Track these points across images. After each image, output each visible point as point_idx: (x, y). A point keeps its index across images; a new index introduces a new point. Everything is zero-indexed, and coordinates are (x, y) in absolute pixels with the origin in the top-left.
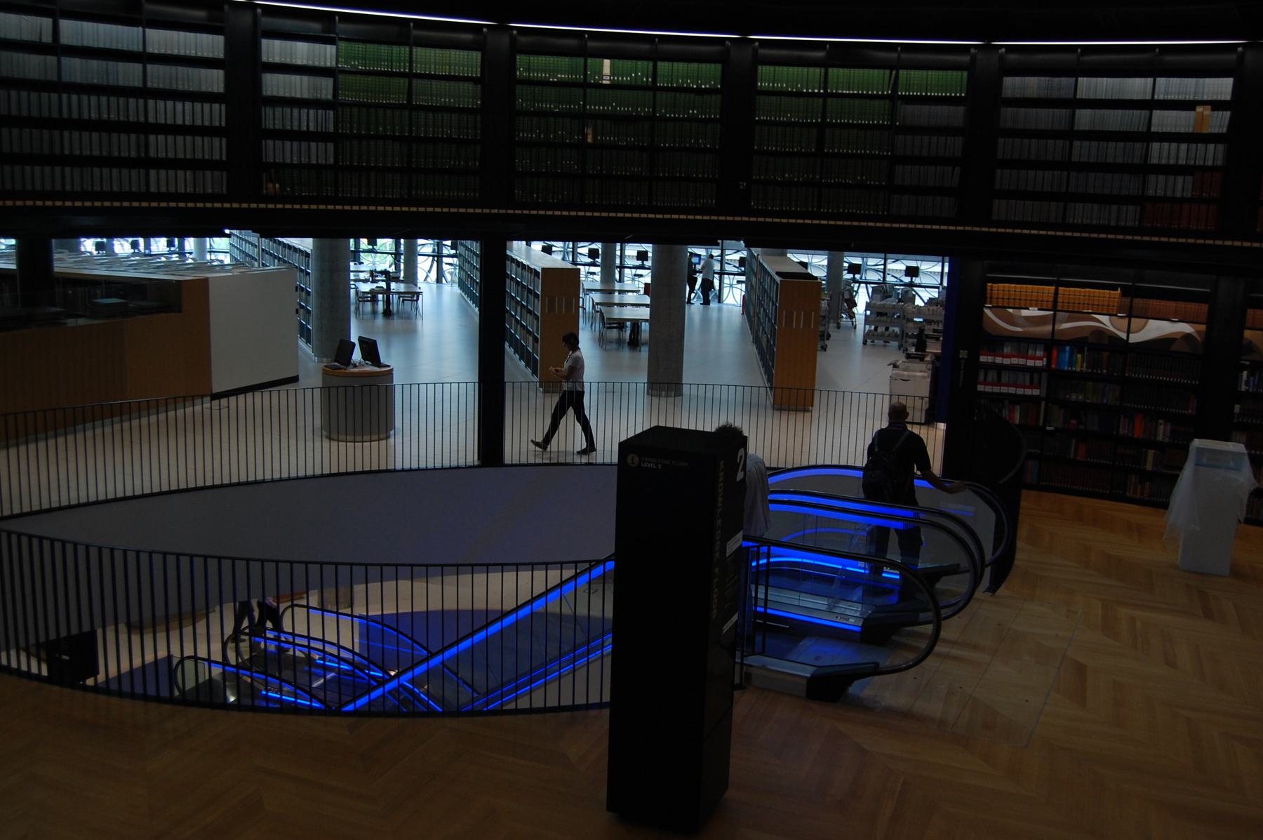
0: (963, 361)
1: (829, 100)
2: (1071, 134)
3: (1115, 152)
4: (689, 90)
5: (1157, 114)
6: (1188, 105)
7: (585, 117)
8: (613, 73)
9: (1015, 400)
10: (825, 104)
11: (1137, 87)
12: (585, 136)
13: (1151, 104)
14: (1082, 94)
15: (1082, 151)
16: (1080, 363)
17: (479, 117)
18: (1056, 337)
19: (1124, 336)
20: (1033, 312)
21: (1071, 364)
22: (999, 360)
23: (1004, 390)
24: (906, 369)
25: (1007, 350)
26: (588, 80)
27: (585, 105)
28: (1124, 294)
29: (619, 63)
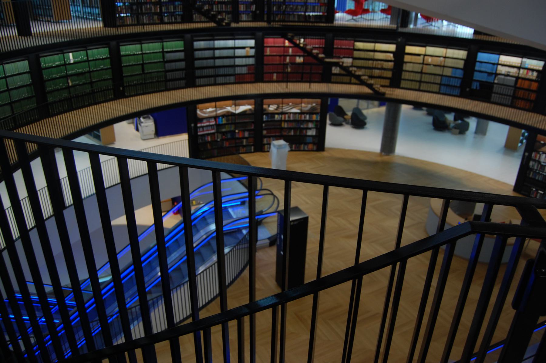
2: (214, 58)
3: (227, 62)
4: (99, 59)
6: (243, 48)
7: (67, 77)
8: (74, 58)
9: (208, 134)
10: (143, 57)
11: (230, 43)
12: (68, 83)
13: (234, 48)
14: (216, 46)
15: (218, 62)
16: (224, 121)
17: (32, 87)
18: (218, 115)
19: (234, 111)
20: (210, 110)
21: (222, 121)
22: (203, 125)
23: (205, 132)
24: (146, 123)
25: (204, 121)
26: (66, 63)
27: (67, 72)
29: (75, 53)
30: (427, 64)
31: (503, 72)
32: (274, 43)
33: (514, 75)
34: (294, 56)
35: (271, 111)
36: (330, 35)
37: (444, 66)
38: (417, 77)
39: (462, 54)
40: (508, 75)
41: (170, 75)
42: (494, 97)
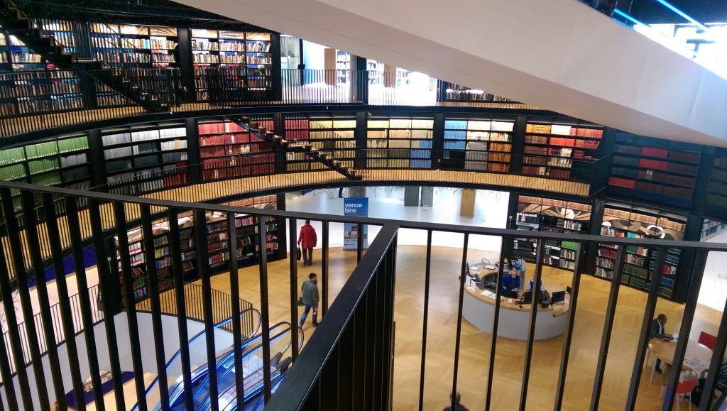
30: (392, 139)
31: (474, 138)
33: (485, 139)
34: (237, 146)
35: (216, 218)
36: (278, 115)
37: (411, 139)
39: (429, 124)
40: (479, 141)
42: (468, 165)
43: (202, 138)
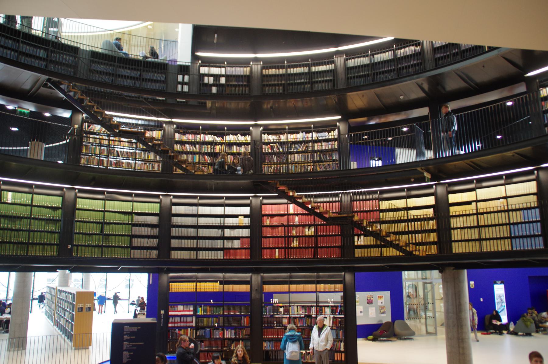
0: (162, 315)
1: (106, 213)
5: (226, 219)
6: (236, 216)
8: (12, 198)
28: (220, 284)
32: (275, 211)
37: (508, 211)
38: (474, 234)
41: (137, 242)
43: (265, 218)
